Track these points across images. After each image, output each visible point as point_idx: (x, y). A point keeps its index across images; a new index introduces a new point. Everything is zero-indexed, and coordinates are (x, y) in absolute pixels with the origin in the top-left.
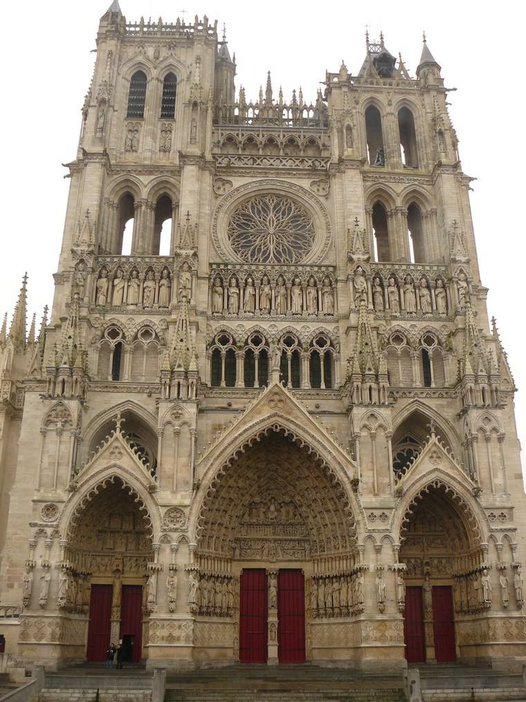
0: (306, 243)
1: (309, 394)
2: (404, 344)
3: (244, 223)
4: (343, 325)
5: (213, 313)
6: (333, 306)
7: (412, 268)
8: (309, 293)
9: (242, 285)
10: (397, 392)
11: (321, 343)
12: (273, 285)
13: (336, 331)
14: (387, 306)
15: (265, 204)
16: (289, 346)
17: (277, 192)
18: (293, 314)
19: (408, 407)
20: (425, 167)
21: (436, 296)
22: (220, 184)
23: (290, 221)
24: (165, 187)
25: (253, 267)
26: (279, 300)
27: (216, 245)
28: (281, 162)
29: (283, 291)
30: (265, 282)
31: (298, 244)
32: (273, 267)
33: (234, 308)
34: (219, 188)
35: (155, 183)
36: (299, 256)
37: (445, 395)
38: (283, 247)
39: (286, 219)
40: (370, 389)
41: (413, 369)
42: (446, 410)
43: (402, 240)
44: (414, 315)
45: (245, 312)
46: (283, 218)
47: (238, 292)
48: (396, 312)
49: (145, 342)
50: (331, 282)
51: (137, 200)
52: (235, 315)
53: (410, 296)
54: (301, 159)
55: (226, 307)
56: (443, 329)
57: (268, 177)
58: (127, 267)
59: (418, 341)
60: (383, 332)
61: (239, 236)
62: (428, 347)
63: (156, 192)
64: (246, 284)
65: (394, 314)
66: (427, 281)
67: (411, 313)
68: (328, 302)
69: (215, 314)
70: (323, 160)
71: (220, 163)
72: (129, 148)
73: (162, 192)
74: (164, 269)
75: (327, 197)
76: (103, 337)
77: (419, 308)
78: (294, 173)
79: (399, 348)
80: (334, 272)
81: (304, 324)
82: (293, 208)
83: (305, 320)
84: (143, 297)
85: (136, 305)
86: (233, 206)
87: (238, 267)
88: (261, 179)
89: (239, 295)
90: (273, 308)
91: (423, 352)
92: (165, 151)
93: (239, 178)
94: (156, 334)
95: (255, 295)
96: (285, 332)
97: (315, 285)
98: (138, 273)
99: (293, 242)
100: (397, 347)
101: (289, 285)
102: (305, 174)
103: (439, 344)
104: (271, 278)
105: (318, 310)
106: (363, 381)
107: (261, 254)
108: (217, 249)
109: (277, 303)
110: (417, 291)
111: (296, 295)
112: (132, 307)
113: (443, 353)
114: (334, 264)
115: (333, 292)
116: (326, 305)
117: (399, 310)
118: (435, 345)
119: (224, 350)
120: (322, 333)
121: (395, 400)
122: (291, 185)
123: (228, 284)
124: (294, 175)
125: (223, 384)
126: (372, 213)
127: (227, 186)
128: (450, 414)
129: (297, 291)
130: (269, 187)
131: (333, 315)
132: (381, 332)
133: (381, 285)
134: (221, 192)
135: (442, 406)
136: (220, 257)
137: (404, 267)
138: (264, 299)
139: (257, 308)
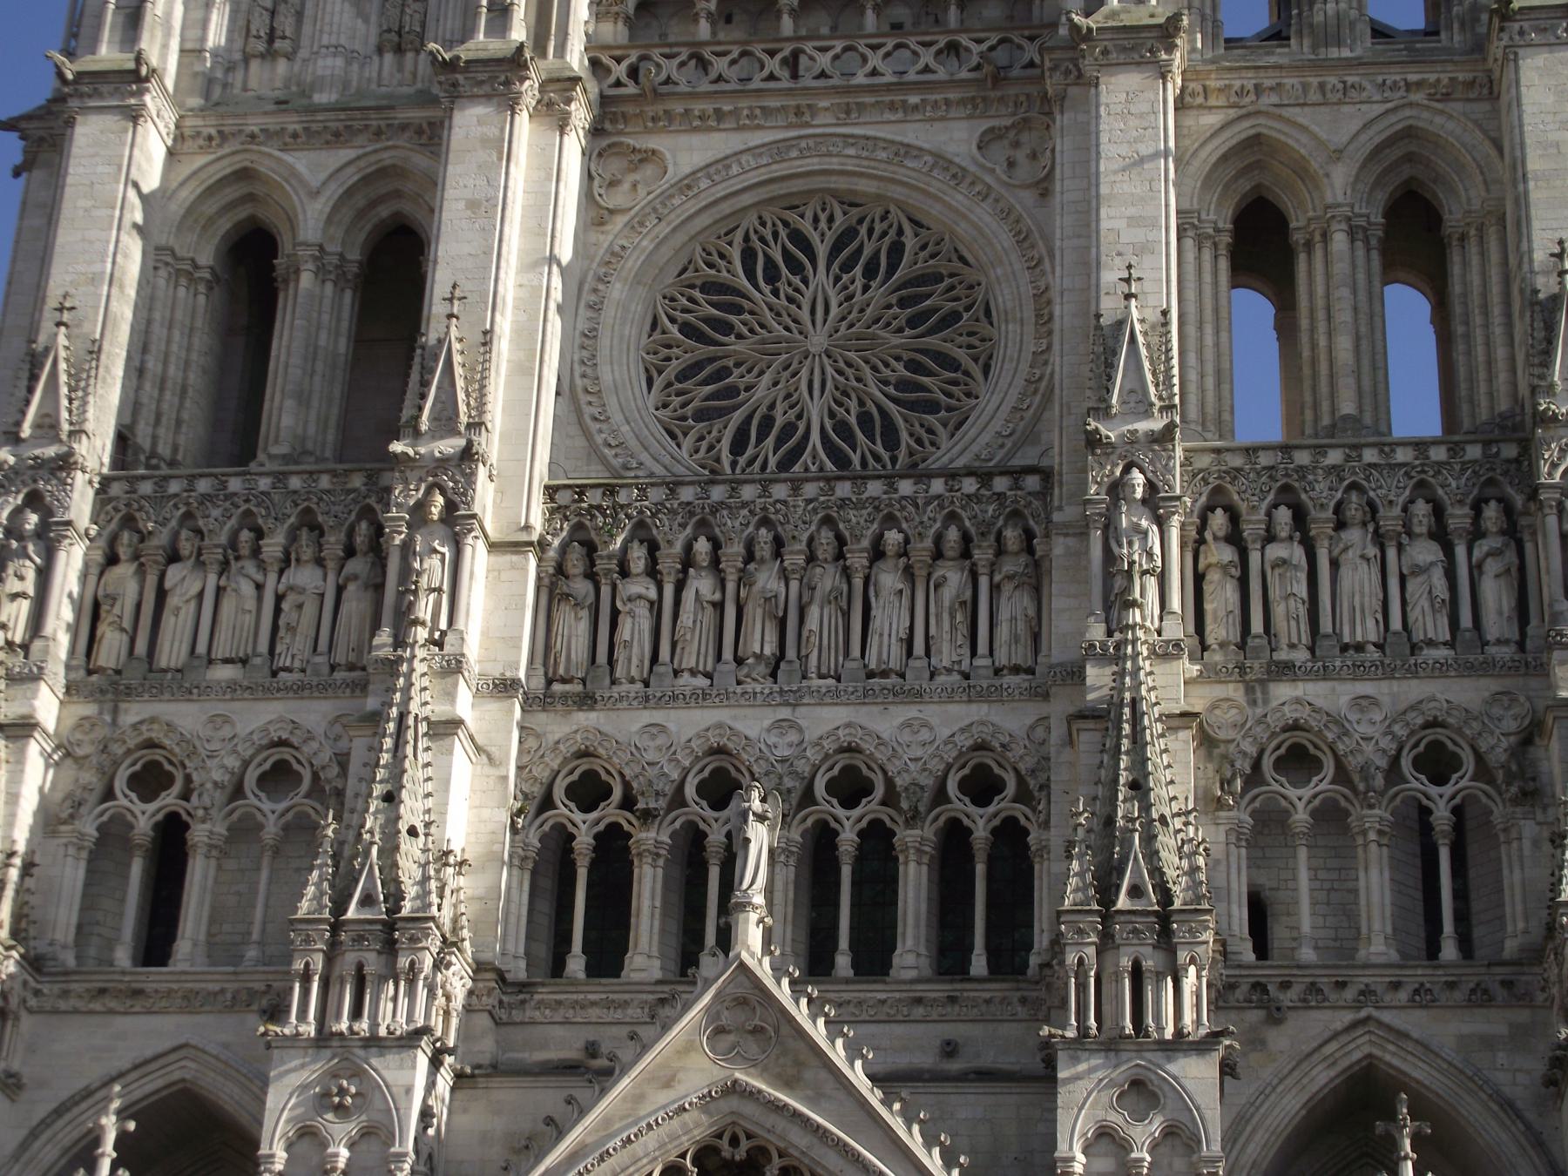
0: (955, 383)
1: (919, 1001)
2: (1323, 783)
3: (708, 320)
4: (1059, 707)
5: (549, 682)
6: (1036, 637)
7: (1370, 456)
8: (936, 587)
9: (669, 563)
10: (1285, 986)
11: (982, 787)
12: (795, 558)
13: (1040, 733)
14: (1257, 626)
15: (798, 238)
16: (849, 802)
17: (841, 184)
18: (871, 675)
19: (1333, 1046)
20: (1462, 25)
21: (1476, 570)
22: (615, 165)
23: (894, 299)
24: (397, 194)
25: (718, 493)
26: (812, 622)
27: (588, 410)
28: (865, 59)
29: (827, 579)
30: (764, 549)
31: (924, 388)
32: (796, 490)
33: (633, 658)
34: (613, 184)
35: (351, 176)
36: (925, 436)
37: (1500, 993)
38: (861, 403)
39: (878, 293)
40: (1137, 974)
41: (1362, 883)
42: (1501, 1058)
43: (1344, 344)
44: (1373, 654)
45: (676, 673)
46: (866, 288)
47: (652, 594)
48: (1292, 646)
49: (271, 811)
50: (1029, 535)
51: (285, 245)
52: (639, 686)
53: (1359, 580)
54: (942, 41)
55: (602, 657)
56: (1496, 711)
57: (807, 125)
58: (216, 513)
59: (1383, 763)
60: (1231, 734)
61: (683, 376)
62: (1433, 790)
63: (361, 214)
64: (688, 561)
65: (1283, 655)
66: (1438, 511)
67: (1359, 648)
68: (1013, 619)
69: (557, 687)
70: (1031, 39)
71: (618, 84)
72: (261, 47)
73: (384, 212)
74: (359, 518)
75: (1044, 188)
76: (109, 794)
77: (1396, 624)
78: (914, 99)
79: (1300, 799)
80: (1044, 493)
81: (911, 712)
82: (910, 242)
83: (917, 696)
84: (275, 628)
85: (244, 662)
86: (666, 252)
87: (656, 494)
88: (781, 135)
89: (656, 607)
90: (791, 653)
91: (1414, 814)
92: (399, 50)
93: (696, 140)
94: (316, 776)
95: (719, 606)
96: (829, 745)
97: (966, 554)
98: (259, 534)
99: (902, 385)
100: (1292, 793)
101: (857, 560)
102: (962, 102)
103: (1483, 771)
104: (785, 532)
105: (974, 653)
106: (1106, 943)
107: (770, 441)
108: (594, 426)
109: (805, 634)
110: (1391, 553)
111: (884, 593)
112: (223, 673)
113: (1499, 812)
114: (1044, 463)
115: (1036, 580)
116: (1003, 632)
117: (1305, 639)
118: (1463, 781)
119: (584, 828)
120: (981, 747)
121: (1275, 1016)
122: (906, 151)
123: (614, 566)
124: (916, 108)
125: (576, 964)
126: (1226, 239)
127: (649, 170)
128: (1521, 1078)
129: (889, 579)
130: (813, 164)
131: (1031, 671)
132: (1222, 735)
133: (1234, 538)
134: (617, 199)
135: (1488, 1043)
136: (603, 461)
137: (1334, 457)
138: (754, 614)
139: (728, 654)
